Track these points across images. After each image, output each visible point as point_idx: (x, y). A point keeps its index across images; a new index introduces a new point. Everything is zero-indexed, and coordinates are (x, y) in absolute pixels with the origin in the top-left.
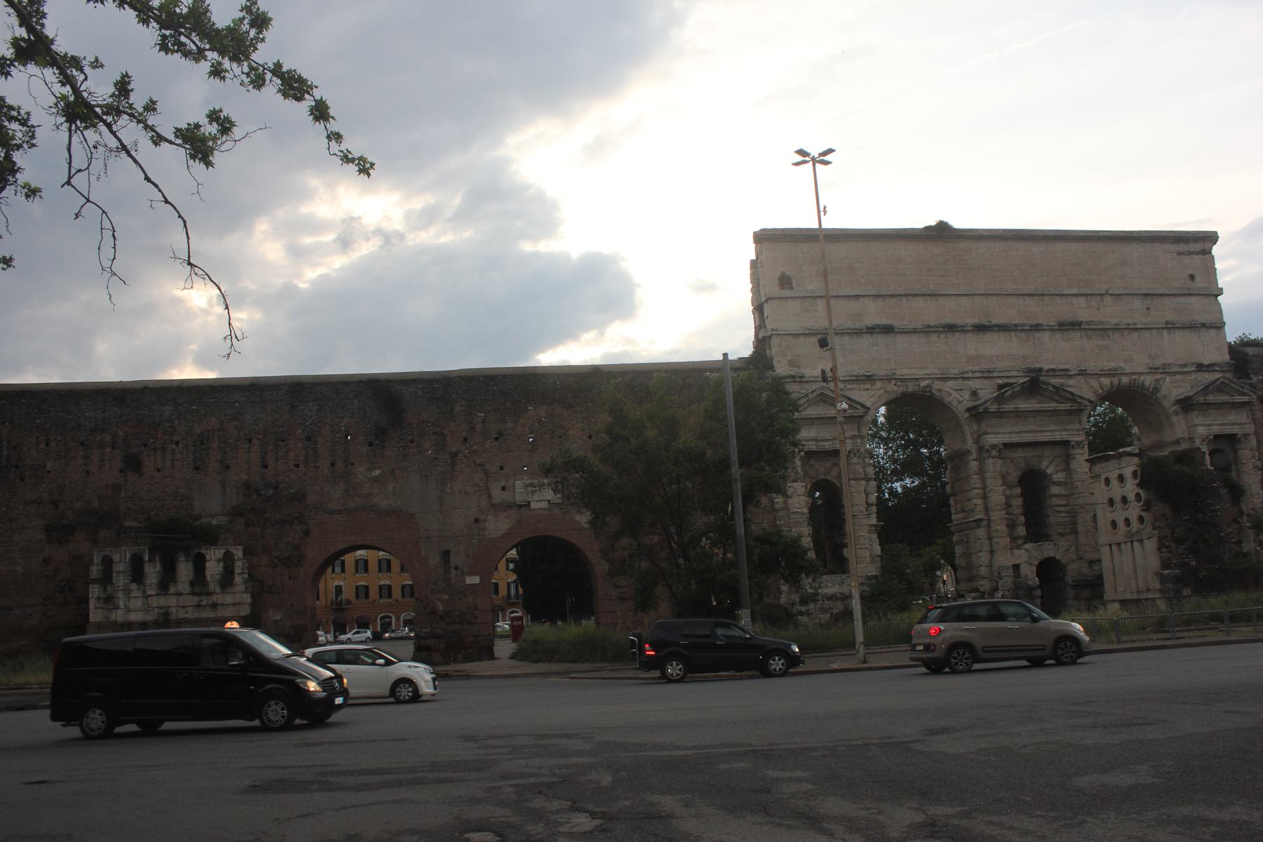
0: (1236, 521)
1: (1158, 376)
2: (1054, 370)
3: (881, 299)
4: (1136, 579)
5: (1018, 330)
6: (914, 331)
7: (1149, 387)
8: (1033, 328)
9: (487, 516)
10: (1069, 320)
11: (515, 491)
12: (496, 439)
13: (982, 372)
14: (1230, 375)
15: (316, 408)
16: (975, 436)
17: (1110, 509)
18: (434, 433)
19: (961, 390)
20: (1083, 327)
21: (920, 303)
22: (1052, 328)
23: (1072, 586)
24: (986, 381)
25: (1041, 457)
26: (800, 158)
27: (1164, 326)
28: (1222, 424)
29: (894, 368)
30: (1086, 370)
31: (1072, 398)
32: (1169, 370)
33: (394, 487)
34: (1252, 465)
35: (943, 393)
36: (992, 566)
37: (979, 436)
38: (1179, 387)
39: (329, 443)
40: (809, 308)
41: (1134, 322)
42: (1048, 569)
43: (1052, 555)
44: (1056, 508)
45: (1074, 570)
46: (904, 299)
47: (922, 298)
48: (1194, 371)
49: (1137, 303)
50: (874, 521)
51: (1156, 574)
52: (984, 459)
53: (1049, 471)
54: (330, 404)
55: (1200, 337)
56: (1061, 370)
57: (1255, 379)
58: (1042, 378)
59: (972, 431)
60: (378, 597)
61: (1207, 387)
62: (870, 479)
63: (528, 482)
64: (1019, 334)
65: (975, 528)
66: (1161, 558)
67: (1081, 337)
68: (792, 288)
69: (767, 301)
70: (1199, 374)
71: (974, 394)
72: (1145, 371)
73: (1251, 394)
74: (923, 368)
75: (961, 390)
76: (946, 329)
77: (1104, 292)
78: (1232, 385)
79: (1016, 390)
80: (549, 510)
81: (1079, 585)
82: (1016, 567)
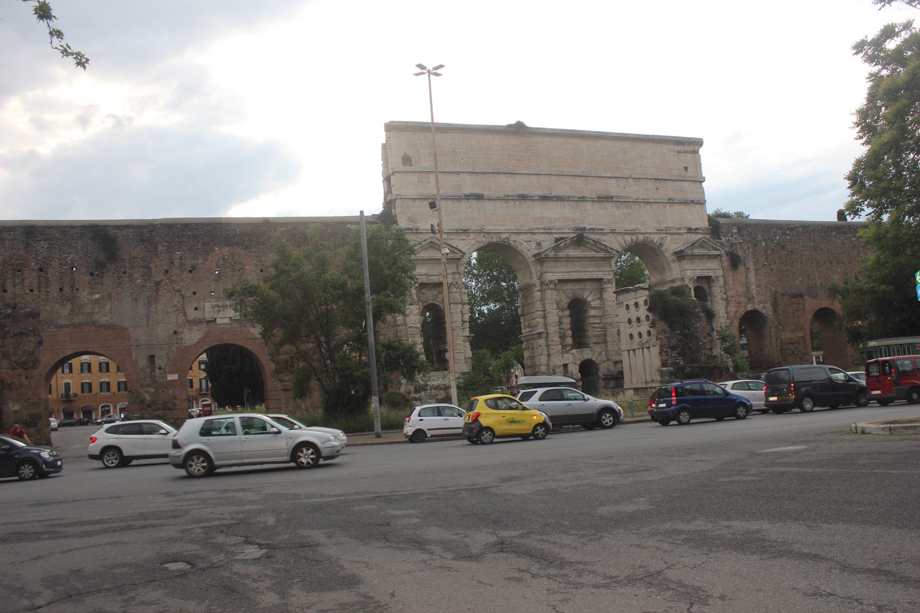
0: (709, 335)
1: (663, 236)
2: (594, 229)
3: (475, 174)
4: (645, 374)
5: (570, 200)
6: (498, 199)
8: (580, 199)
9: (183, 329)
10: (605, 195)
11: (204, 310)
12: (191, 271)
13: (545, 229)
14: (708, 236)
15: (47, 245)
16: (539, 274)
17: (629, 326)
18: (141, 267)
19: (530, 241)
20: (613, 200)
21: (502, 179)
22: (593, 199)
23: (602, 379)
24: (547, 236)
25: (583, 289)
26: (419, 71)
27: (667, 201)
28: (703, 269)
29: (483, 224)
30: (615, 230)
31: (605, 249)
32: (669, 232)
33: (111, 307)
34: (720, 297)
35: (517, 243)
36: (549, 365)
37: (541, 274)
38: (676, 243)
39: (58, 273)
40: (424, 180)
41: (648, 197)
42: (587, 368)
43: (590, 358)
44: (593, 325)
45: (604, 368)
46: (491, 176)
47: (504, 175)
48: (687, 233)
49: (651, 185)
50: (467, 333)
51: (658, 370)
52: (545, 291)
53: (589, 300)
54: (58, 243)
55: (690, 210)
56: (598, 229)
57: (724, 240)
58: (585, 235)
59: (537, 271)
60: (99, 391)
61: (693, 244)
62: (465, 304)
63: (214, 304)
64: (570, 203)
65: (537, 339)
66: (661, 359)
67: (613, 207)
68: (411, 165)
69: (393, 174)
70: (689, 235)
71: (539, 244)
73: (721, 249)
74: (503, 225)
75: (530, 241)
76: (520, 198)
77: (628, 176)
78: (709, 243)
79: (567, 242)
80: (231, 325)
81: (607, 378)
82: (565, 366)
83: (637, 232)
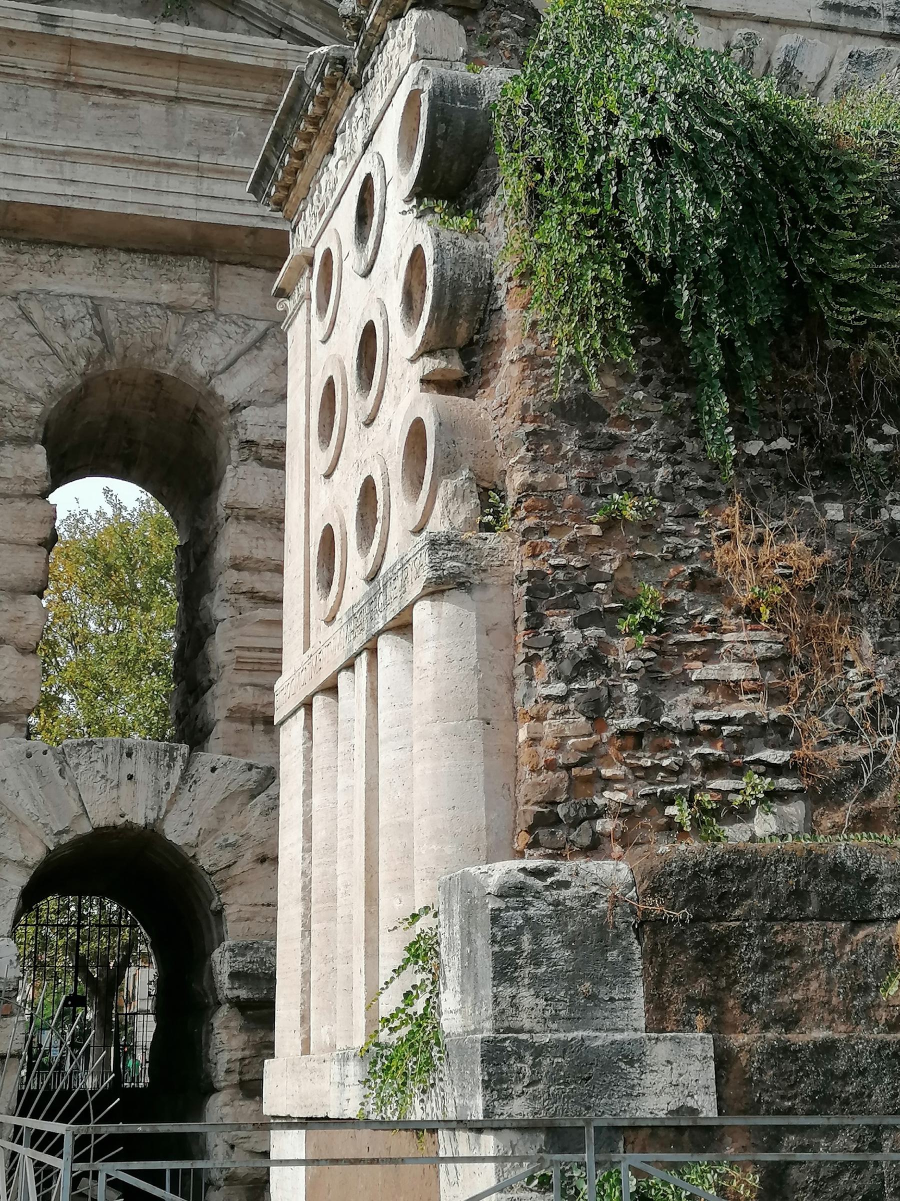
72: (802, 16)
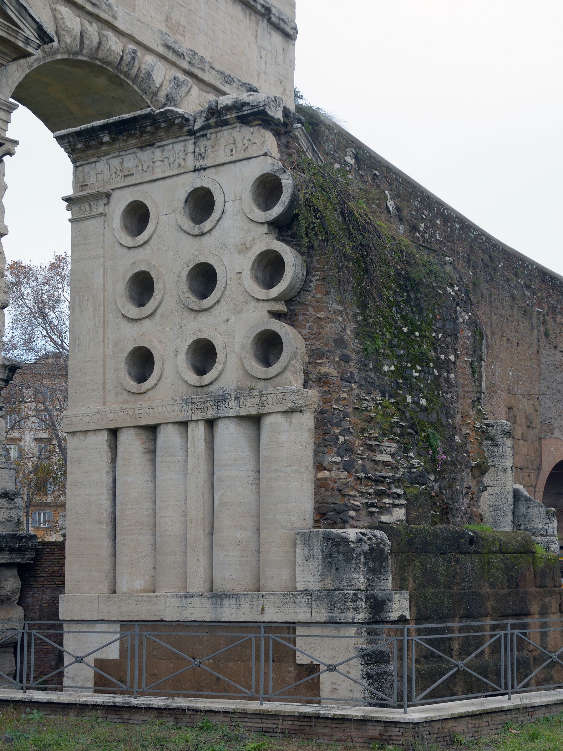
7: (159, 89)
32: (199, 74)
51: (307, 540)
72: (154, 47)
83: (103, 15)
